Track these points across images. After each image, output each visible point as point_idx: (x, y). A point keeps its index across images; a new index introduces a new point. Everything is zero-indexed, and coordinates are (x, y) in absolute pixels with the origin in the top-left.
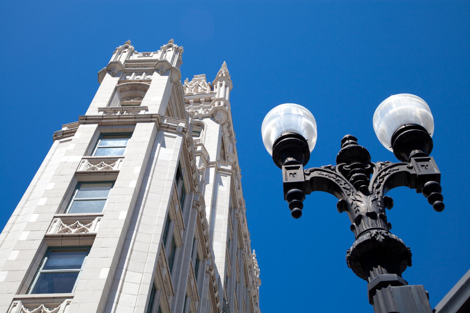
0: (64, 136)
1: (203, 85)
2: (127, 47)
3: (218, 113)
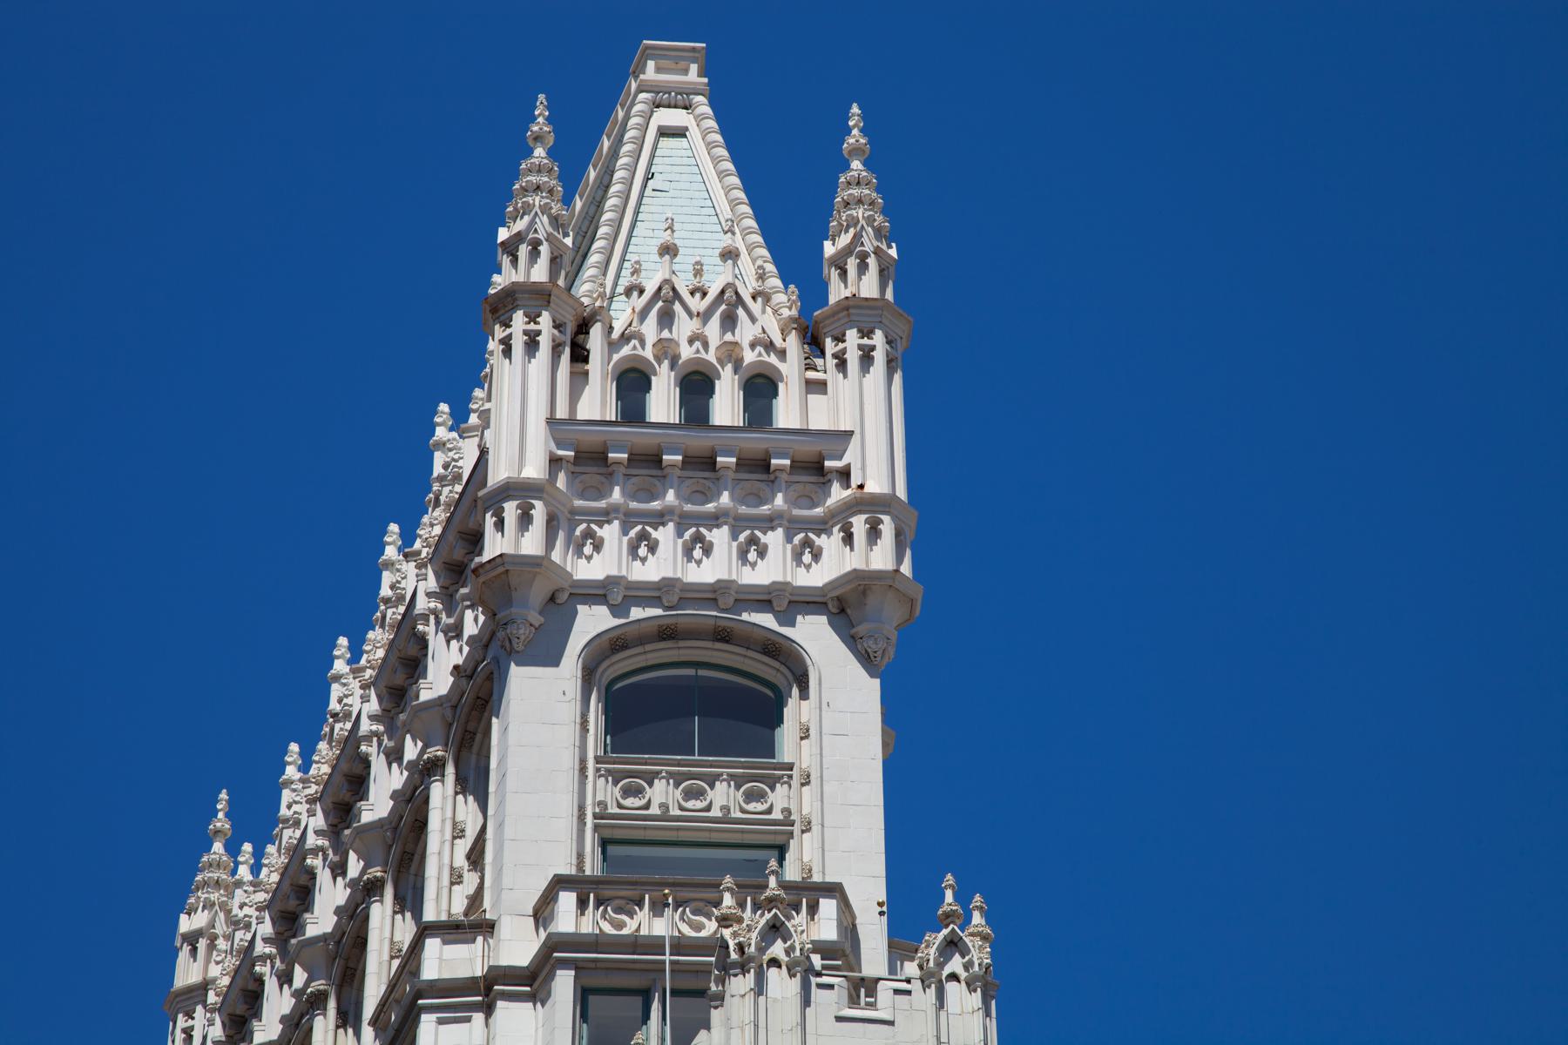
1: (759, 300)
2: (778, 924)
3: (872, 601)
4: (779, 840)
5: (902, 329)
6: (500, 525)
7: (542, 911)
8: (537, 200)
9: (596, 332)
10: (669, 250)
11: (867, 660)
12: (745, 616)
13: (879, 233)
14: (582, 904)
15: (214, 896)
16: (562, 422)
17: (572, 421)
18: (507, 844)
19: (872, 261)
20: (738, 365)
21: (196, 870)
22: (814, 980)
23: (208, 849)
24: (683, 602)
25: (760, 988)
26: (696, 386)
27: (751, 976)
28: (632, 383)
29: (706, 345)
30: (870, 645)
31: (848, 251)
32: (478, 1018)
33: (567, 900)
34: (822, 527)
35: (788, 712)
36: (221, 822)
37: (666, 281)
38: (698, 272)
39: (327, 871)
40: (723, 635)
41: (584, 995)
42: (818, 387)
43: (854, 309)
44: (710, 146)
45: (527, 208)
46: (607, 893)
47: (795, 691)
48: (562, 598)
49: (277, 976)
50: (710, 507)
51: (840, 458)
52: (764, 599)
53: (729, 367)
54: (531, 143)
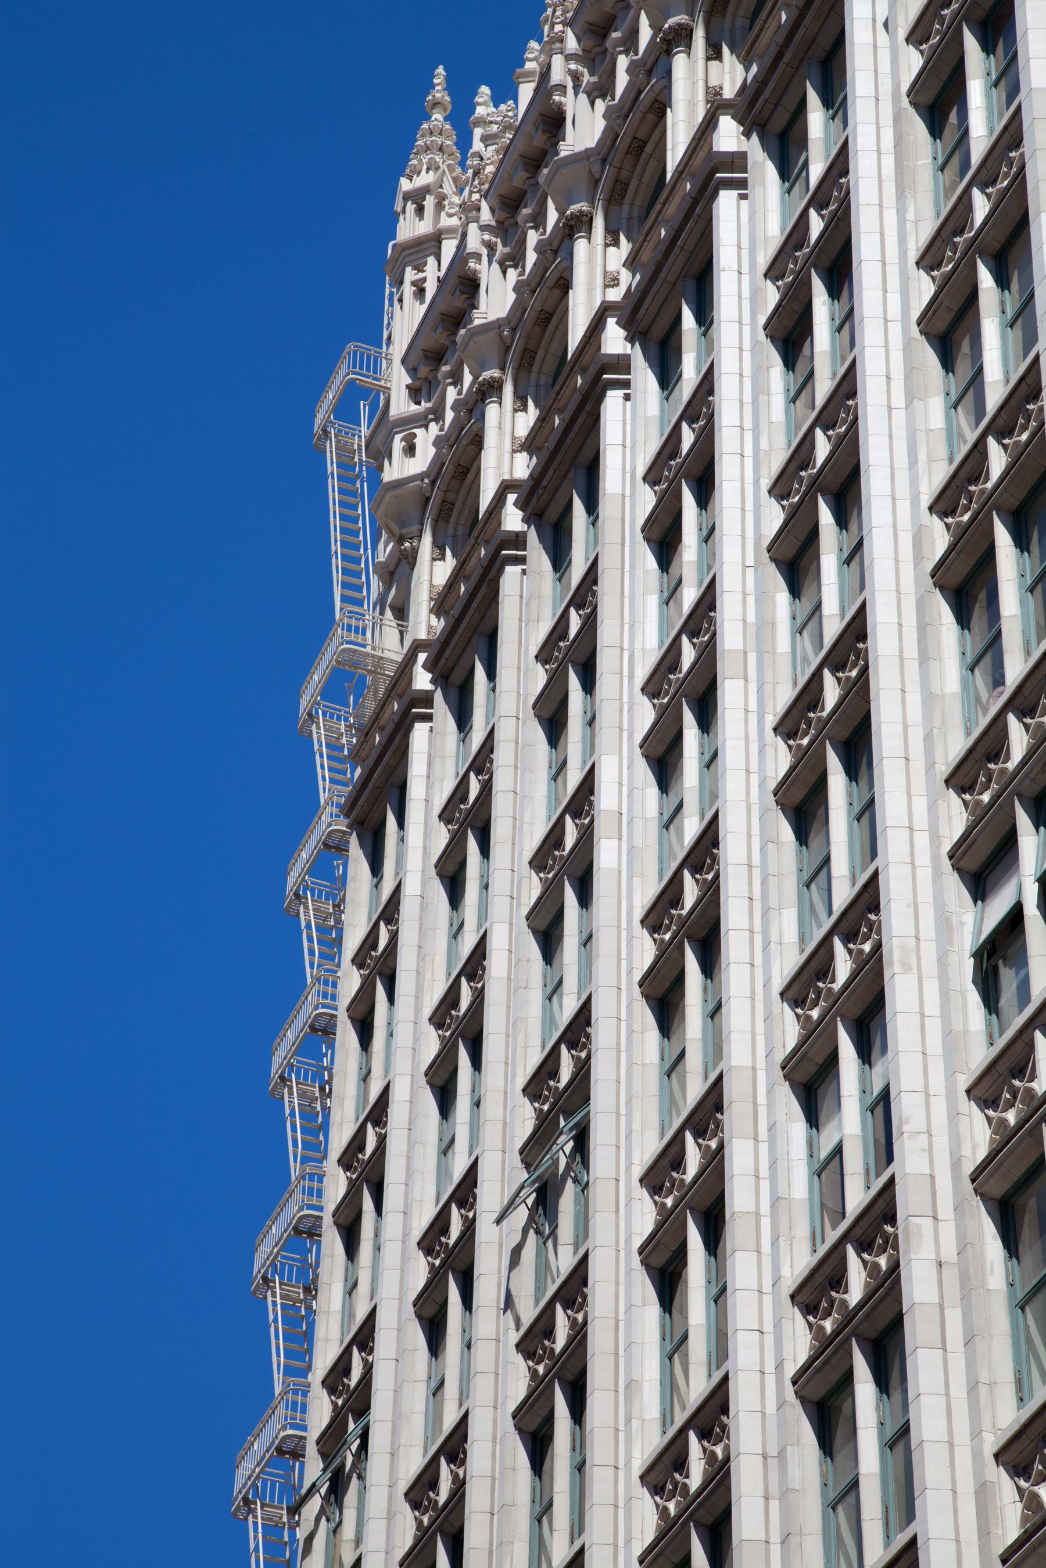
23: (428, 118)
49: (584, 92)
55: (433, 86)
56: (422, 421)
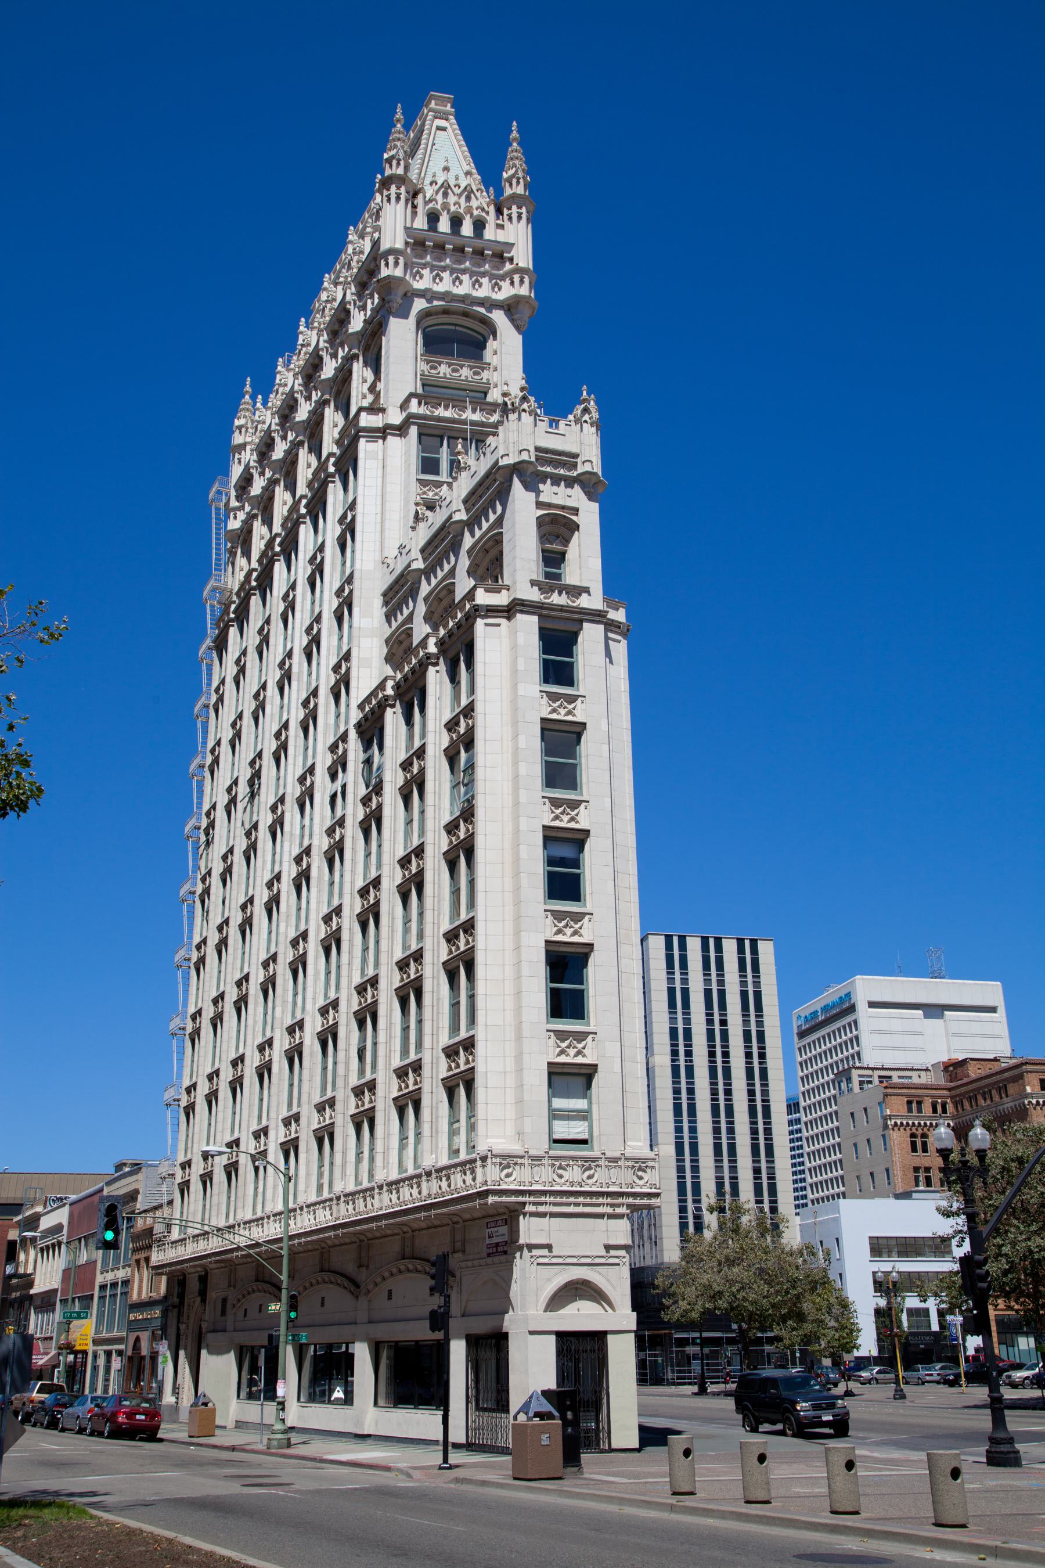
0: (489, 614)
3: (521, 307)
4: (485, 390)
5: (532, 208)
6: (387, 265)
7: (404, 405)
8: (398, 144)
9: (420, 196)
10: (446, 169)
11: (518, 328)
12: (474, 308)
13: (523, 170)
14: (420, 404)
15: (247, 414)
16: (408, 228)
17: (412, 228)
18: (390, 382)
19: (521, 181)
20: (472, 215)
21: (240, 405)
22: (538, 418)
23: (244, 397)
24: (452, 301)
25: (519, 419)
26: (456, 222)
27: (516, 415)
28: (433, 218)
29: (460, 207)
30: (519, 323)
31: (513, 176)
32: (380, 441)
33: (414, 402)
34: (503, 278)
35: (488, 345)
36: (248, 388)
37: (446, 181)
38: (457, 179)
39: (303, 399)
40: (466, 314)
41: (420, 435)
42: (501, 227)
43: (514, 198)
44: (456, 135)
45: (395, 147)
46: (428, 400)
47: (491, 337)
48: (409, 294)
50: (462, 266)
51: (509, 253)
52: (481, 302)
53: (469, 215)
54: (395, 122)
55: (246, 385)
56: (239, 509)
